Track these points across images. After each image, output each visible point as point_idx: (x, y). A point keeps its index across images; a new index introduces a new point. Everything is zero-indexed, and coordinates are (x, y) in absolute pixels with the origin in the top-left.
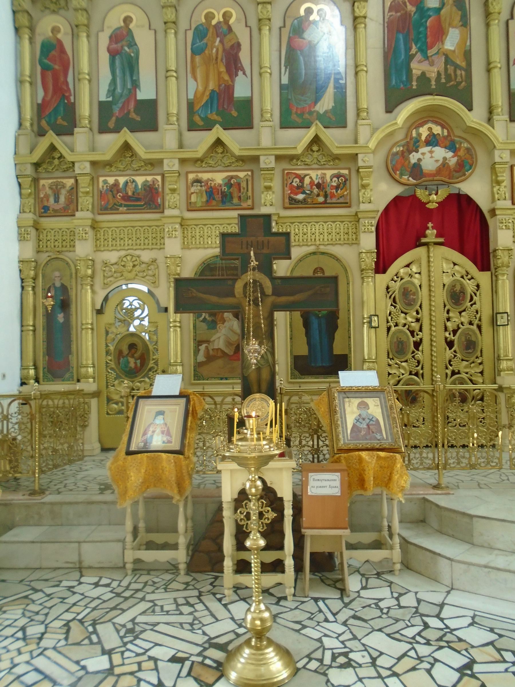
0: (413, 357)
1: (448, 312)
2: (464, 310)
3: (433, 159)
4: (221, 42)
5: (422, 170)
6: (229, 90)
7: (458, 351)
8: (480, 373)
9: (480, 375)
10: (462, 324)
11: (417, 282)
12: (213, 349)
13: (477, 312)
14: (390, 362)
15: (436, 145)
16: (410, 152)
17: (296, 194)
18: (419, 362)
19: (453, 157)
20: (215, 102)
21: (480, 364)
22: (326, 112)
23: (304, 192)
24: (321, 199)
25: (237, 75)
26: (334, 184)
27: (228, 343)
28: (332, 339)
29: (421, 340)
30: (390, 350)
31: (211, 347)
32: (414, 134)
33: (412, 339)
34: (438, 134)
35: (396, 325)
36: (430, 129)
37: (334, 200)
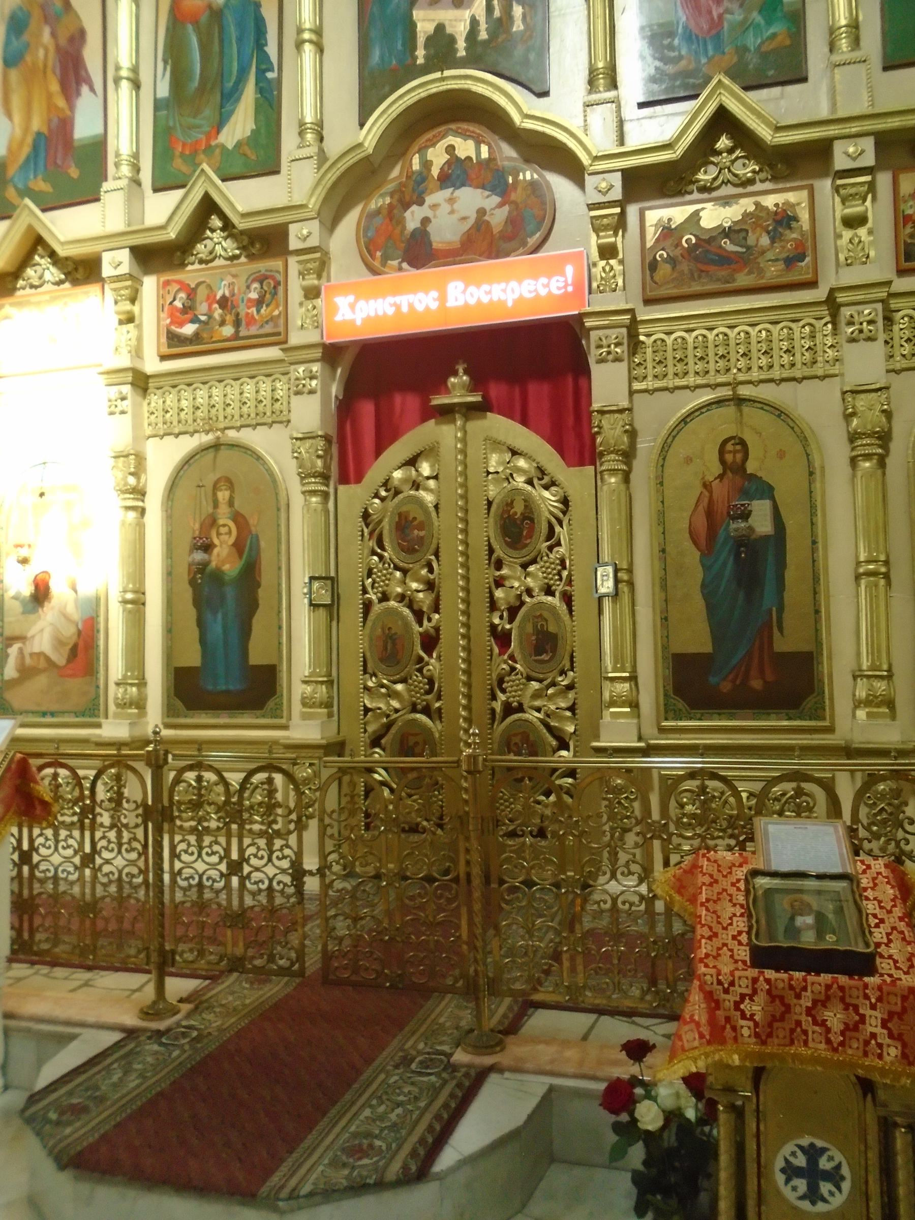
0: (420, 670)
1: (499, 565)
2: (534, 561)
3: (456, 216)
4: (53, 35)
5: (431, 245)
6: (65, 125)
7: (518, 656)
8: (568, 709)
9: (568, 714)
10: (529, 592)
11: (429, 498)
12: (32, 655)
13: (563, 562)
14: (370, 684)
15: (463, 185)
16: (406, 206)
17: (181, 325)
18: (431, 682)
19: (501, 205)
20: (42, 154)
21: (570, 687)
22: (239, 145)
23: (195, 320)
24: (228, 331)
25: (78, 94)
26: (254, 295)
27: (59, 642)
28: (246, 631)
29: (437, 629)
30: (368, 655)
31: (27, 652)
32: (416, 164)
33: (417, 628)
34: (469, 158)
35: (384, 598)
36: (450, 149)
37: (253, 330)
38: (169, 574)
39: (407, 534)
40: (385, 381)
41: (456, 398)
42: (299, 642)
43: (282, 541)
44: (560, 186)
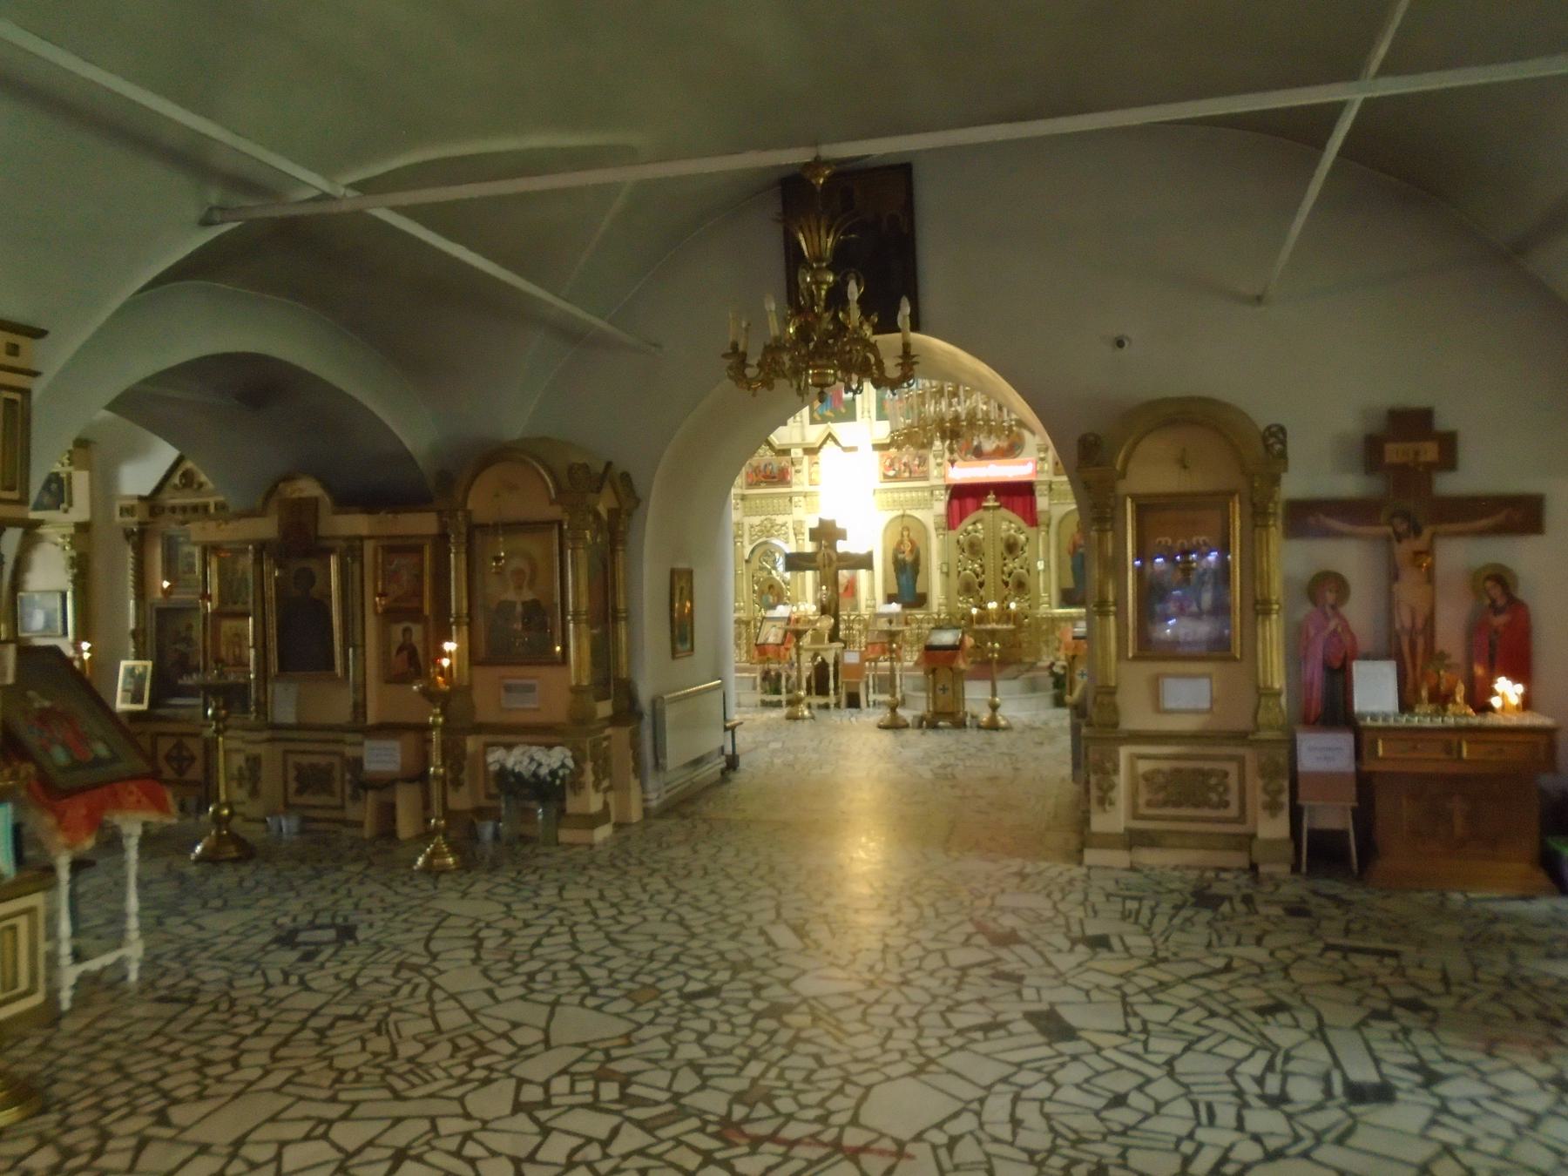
38: (885, 560)
39: (974, 548)
40: (964, 497)
41: (991, 504)
42: (936, 585)
43: (928, 549)
44: (1027, 434)
